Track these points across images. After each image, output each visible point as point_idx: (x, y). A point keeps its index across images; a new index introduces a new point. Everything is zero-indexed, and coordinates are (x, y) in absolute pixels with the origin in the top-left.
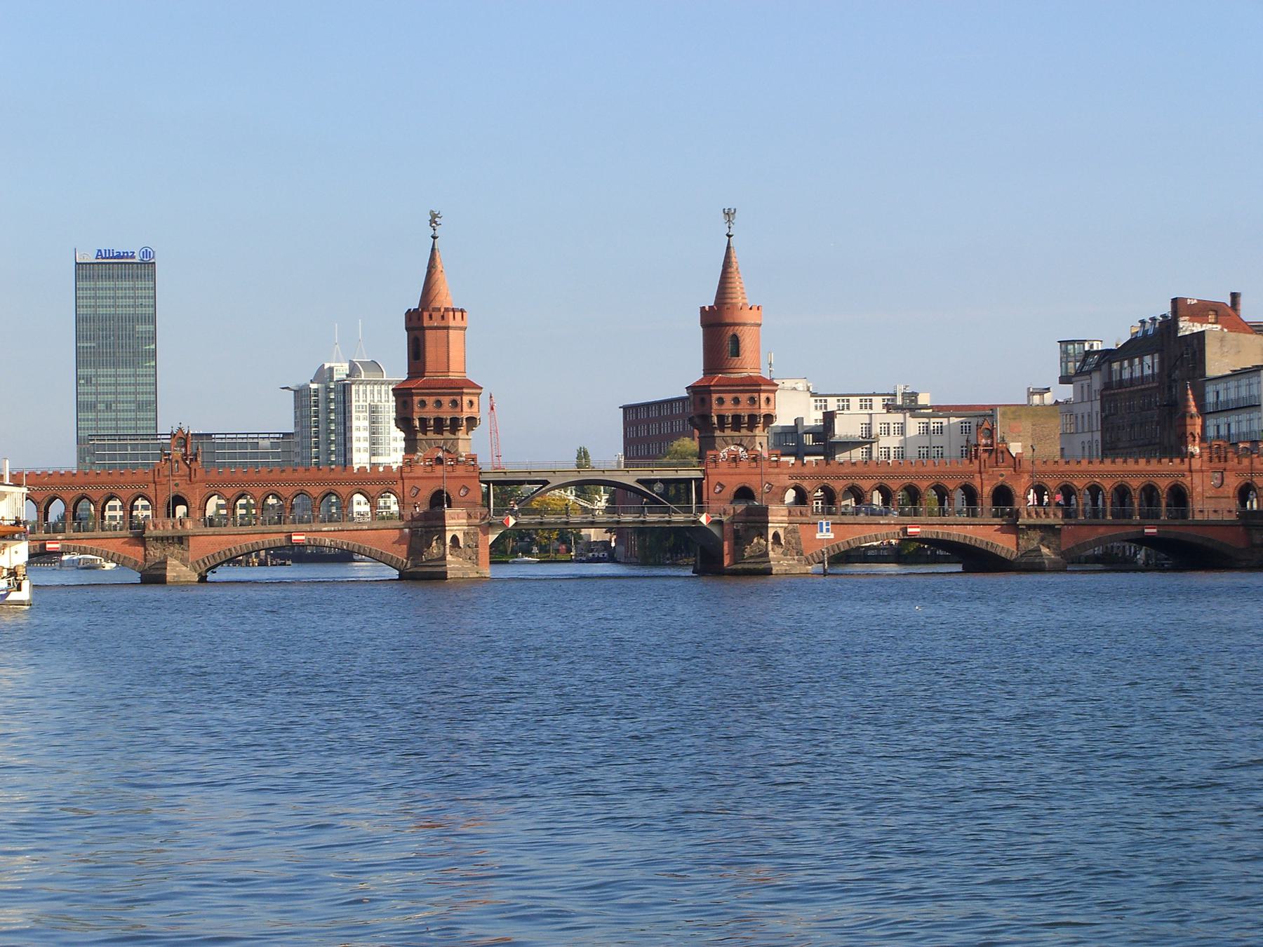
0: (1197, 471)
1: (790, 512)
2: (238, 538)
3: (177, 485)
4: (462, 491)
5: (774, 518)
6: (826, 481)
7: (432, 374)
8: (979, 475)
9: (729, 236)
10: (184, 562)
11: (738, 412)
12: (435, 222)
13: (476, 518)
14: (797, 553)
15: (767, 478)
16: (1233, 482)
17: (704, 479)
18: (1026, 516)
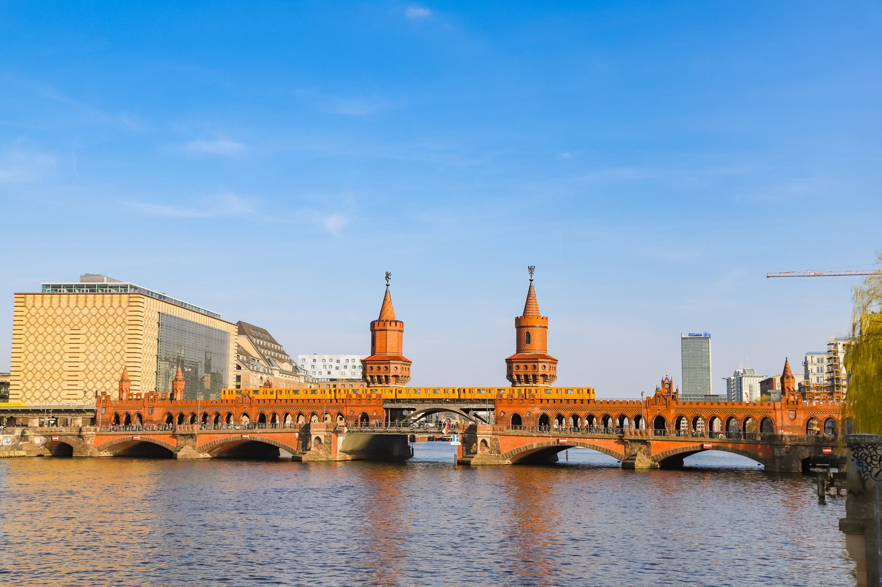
0: (778, 410)
1: (493, 428)
2: (219, 436)
3: (245, 408)
4: (374, 413)
5: (481, 431)
6: (560, 411)
7: (379, 354)
8: (646, 409)
9: (531, 280)
10: (194, 447)
11: (527, 373)
12: (388, 278)
13: (330, 428)
14: (497, 452)
15: (529, 409)
16: (802, 417)
17: (495, 409)
18: (629, 434)
